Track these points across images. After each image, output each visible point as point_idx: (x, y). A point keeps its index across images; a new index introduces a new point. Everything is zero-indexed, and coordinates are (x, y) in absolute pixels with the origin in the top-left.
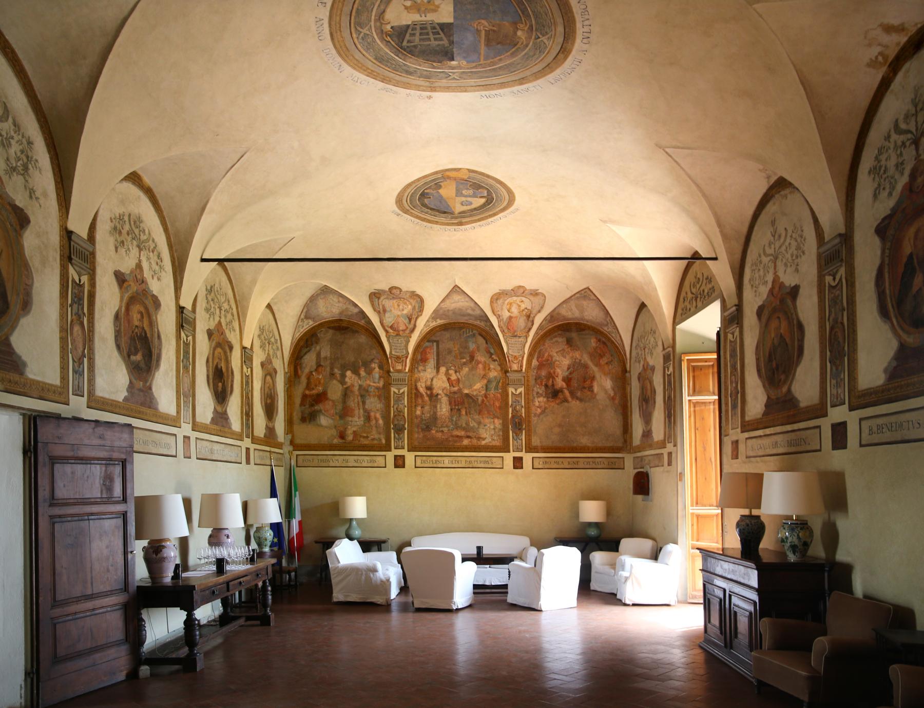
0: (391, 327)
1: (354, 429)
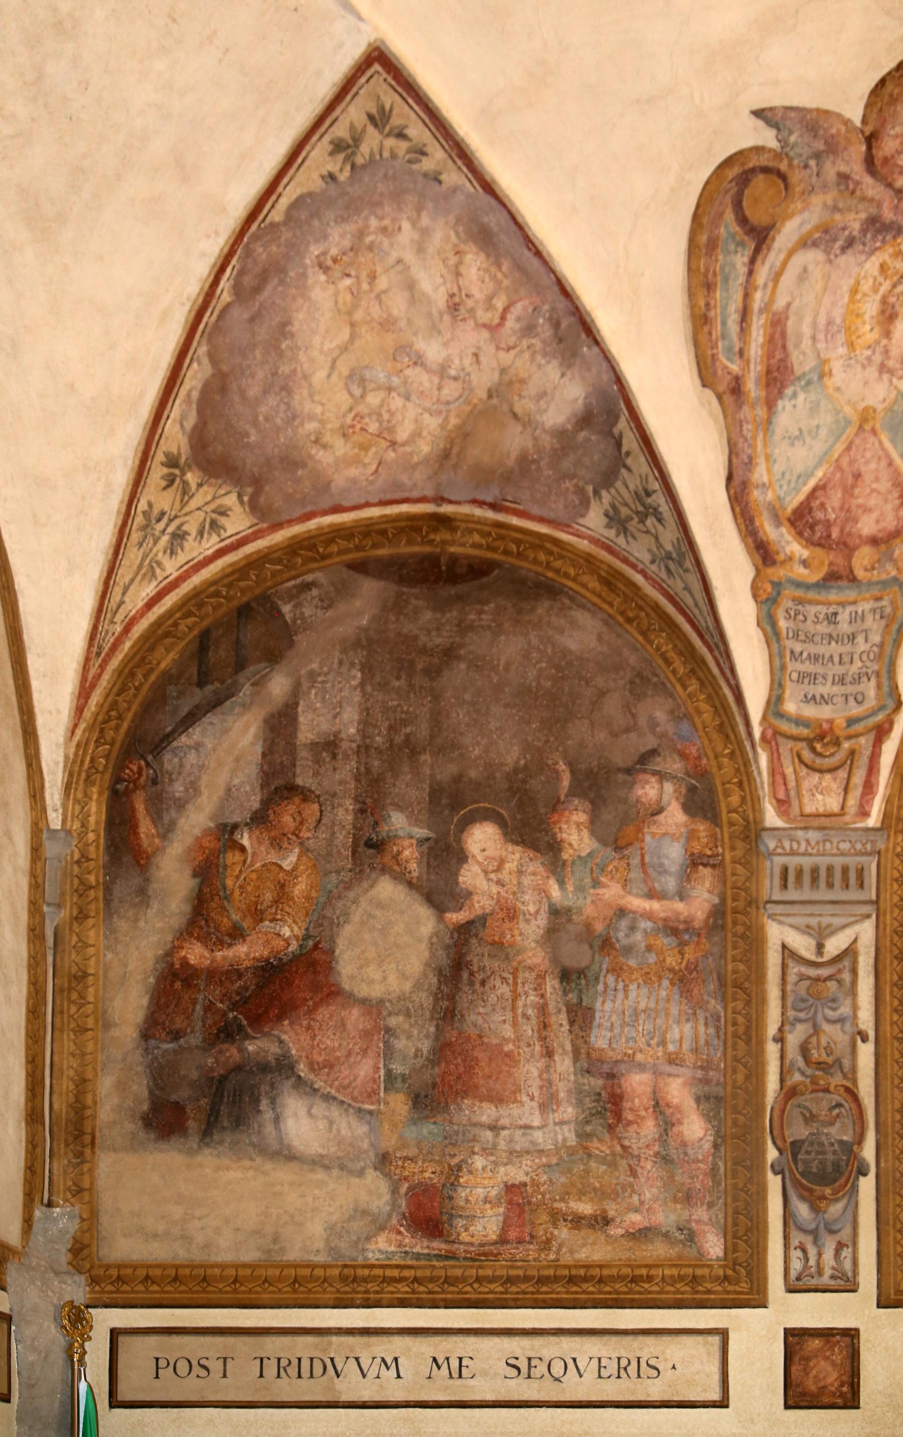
1: (517, 1174)
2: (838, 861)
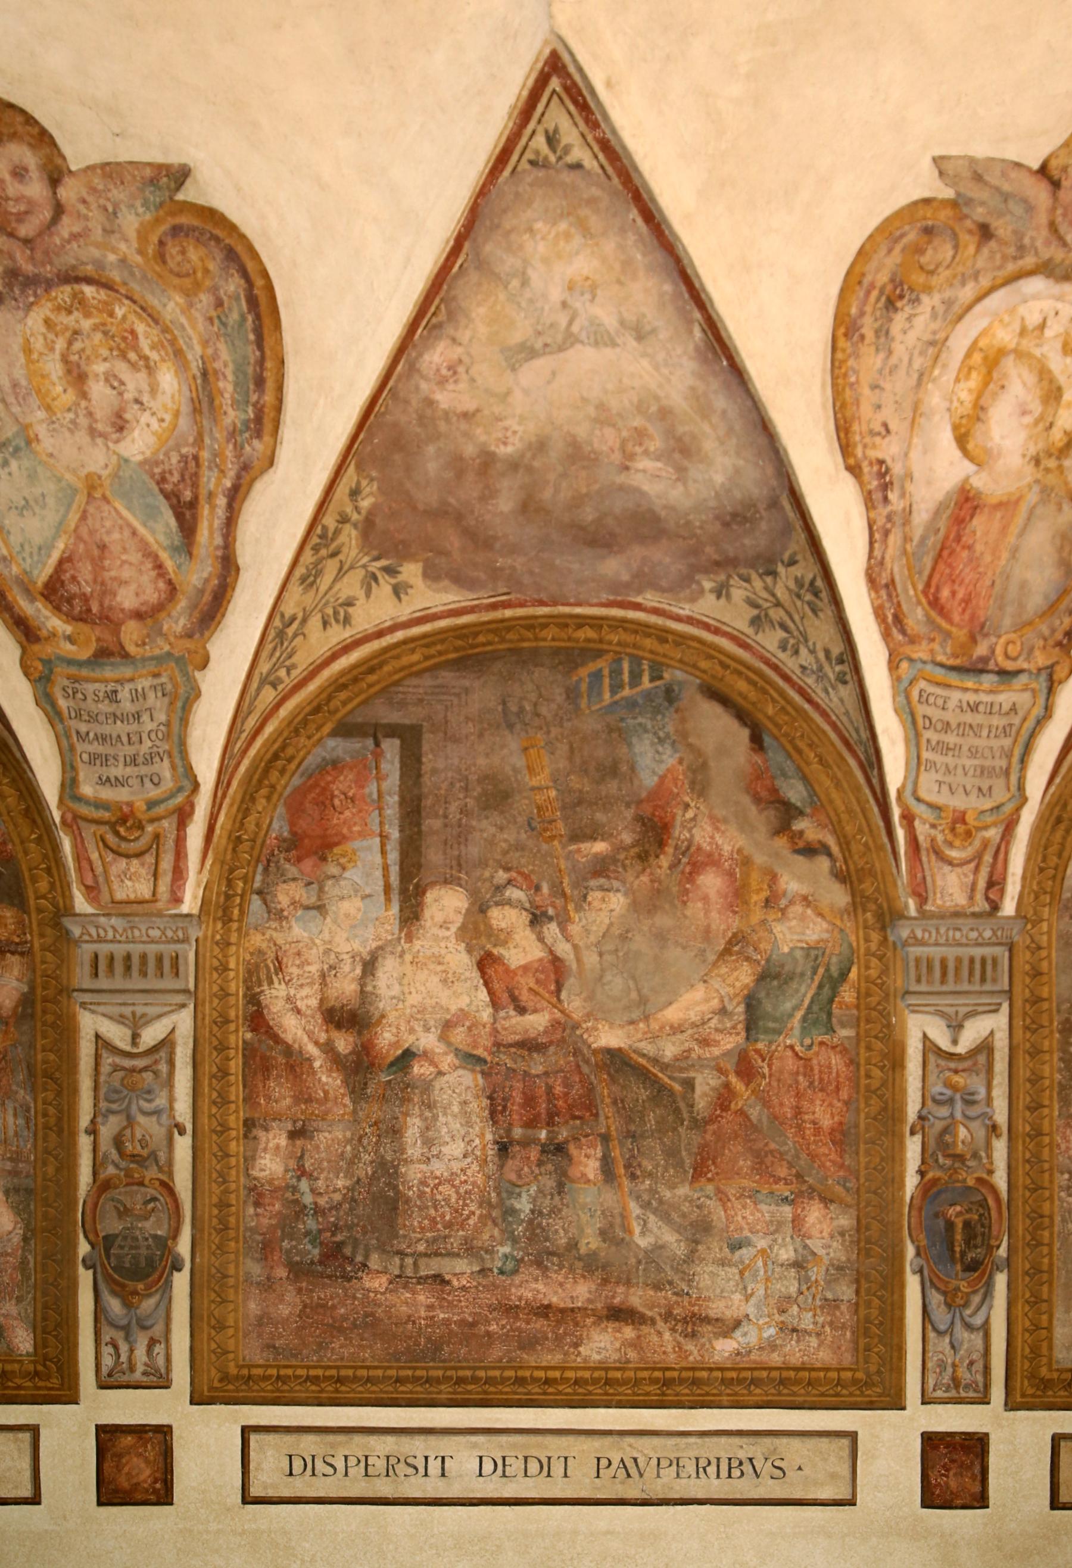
0: (54, 591)
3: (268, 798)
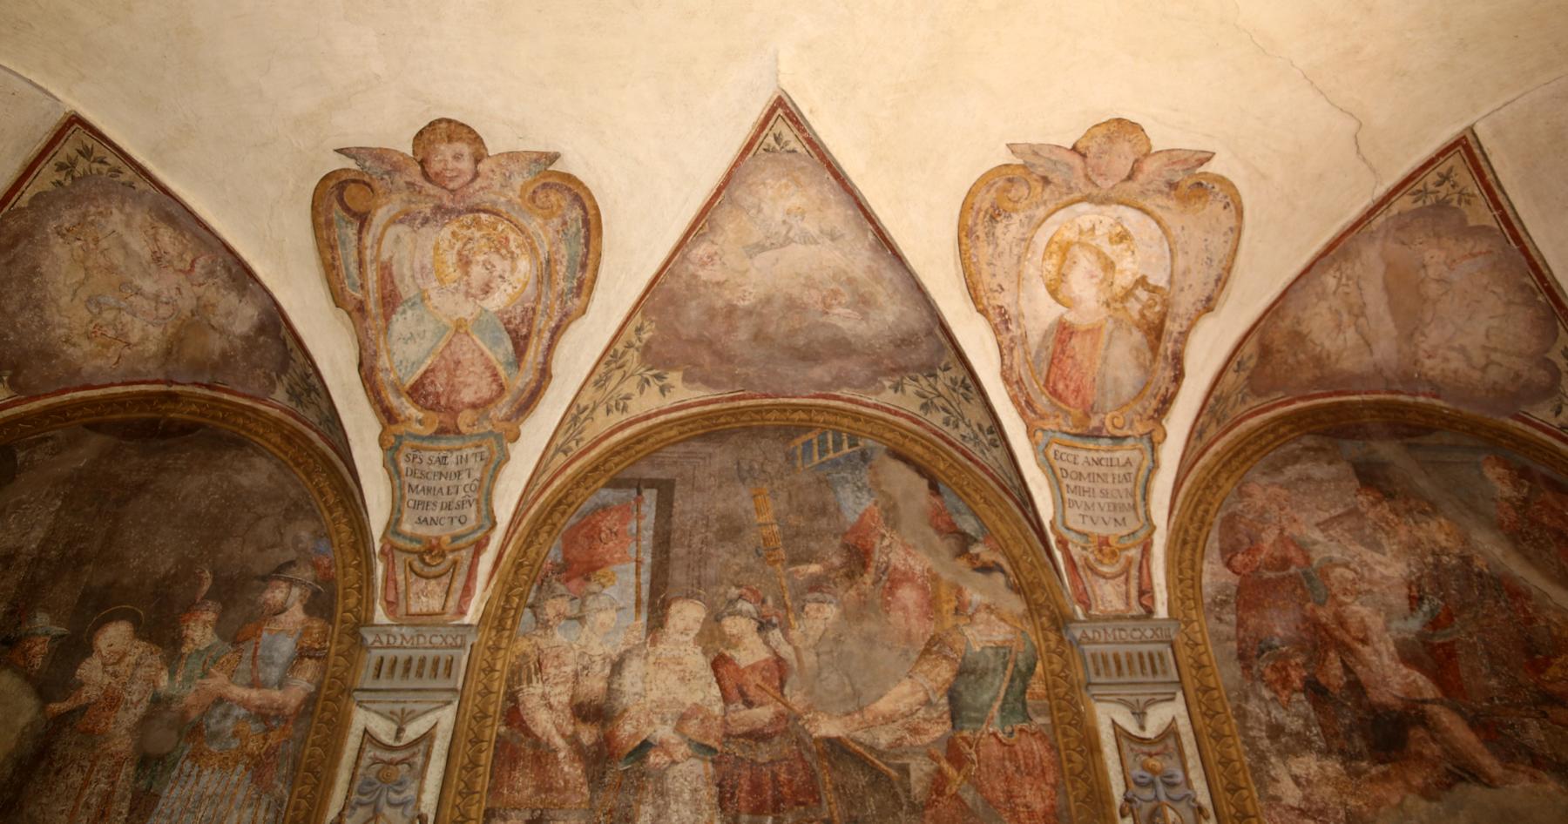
0: (416, 392)
2: (431, 654)
3: (549, 533)
